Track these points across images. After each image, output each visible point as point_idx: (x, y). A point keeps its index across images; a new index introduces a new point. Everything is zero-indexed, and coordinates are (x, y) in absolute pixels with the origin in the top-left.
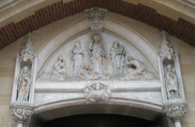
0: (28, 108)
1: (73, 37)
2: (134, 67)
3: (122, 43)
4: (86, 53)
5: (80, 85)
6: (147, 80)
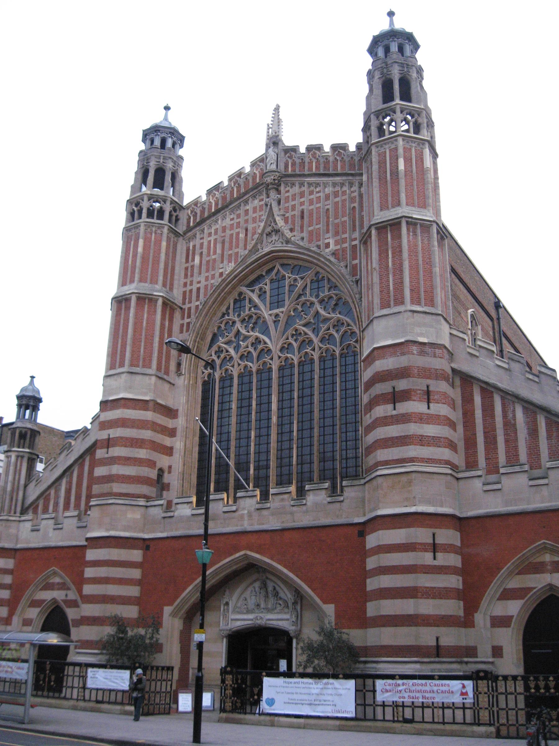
0: (227, 630)
1: (251, 584)
2: (280, 604)
3: (277, 588)
4: (258, 593)
5: (251, 616)
6: (285, 613)
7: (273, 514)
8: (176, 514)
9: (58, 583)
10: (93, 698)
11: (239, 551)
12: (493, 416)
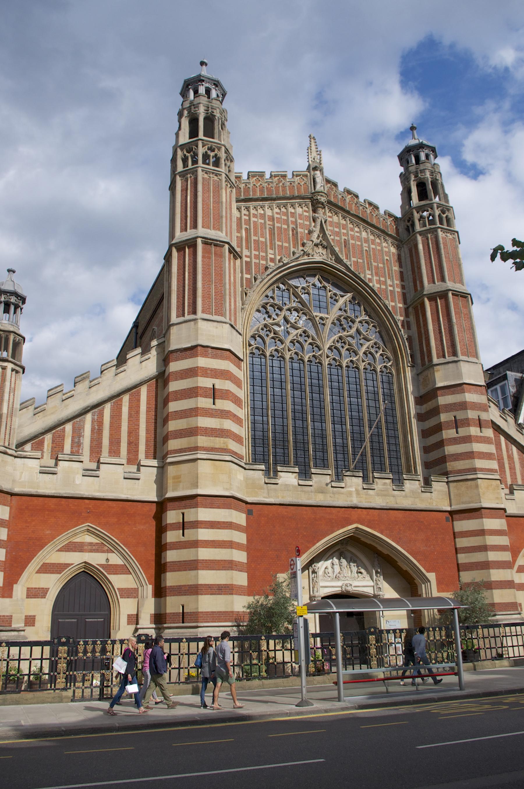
5: (339, 583)
7: (378, 495)
8: (279, 481)
9: (91, 544)
10: (489, 656)
11: (351, 524)
12: (501, 450)
